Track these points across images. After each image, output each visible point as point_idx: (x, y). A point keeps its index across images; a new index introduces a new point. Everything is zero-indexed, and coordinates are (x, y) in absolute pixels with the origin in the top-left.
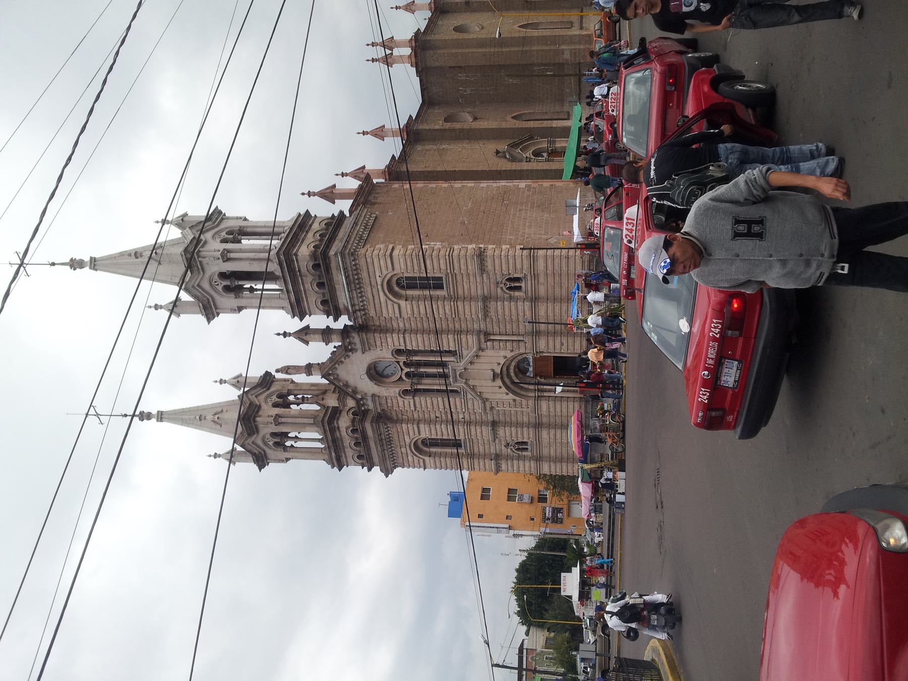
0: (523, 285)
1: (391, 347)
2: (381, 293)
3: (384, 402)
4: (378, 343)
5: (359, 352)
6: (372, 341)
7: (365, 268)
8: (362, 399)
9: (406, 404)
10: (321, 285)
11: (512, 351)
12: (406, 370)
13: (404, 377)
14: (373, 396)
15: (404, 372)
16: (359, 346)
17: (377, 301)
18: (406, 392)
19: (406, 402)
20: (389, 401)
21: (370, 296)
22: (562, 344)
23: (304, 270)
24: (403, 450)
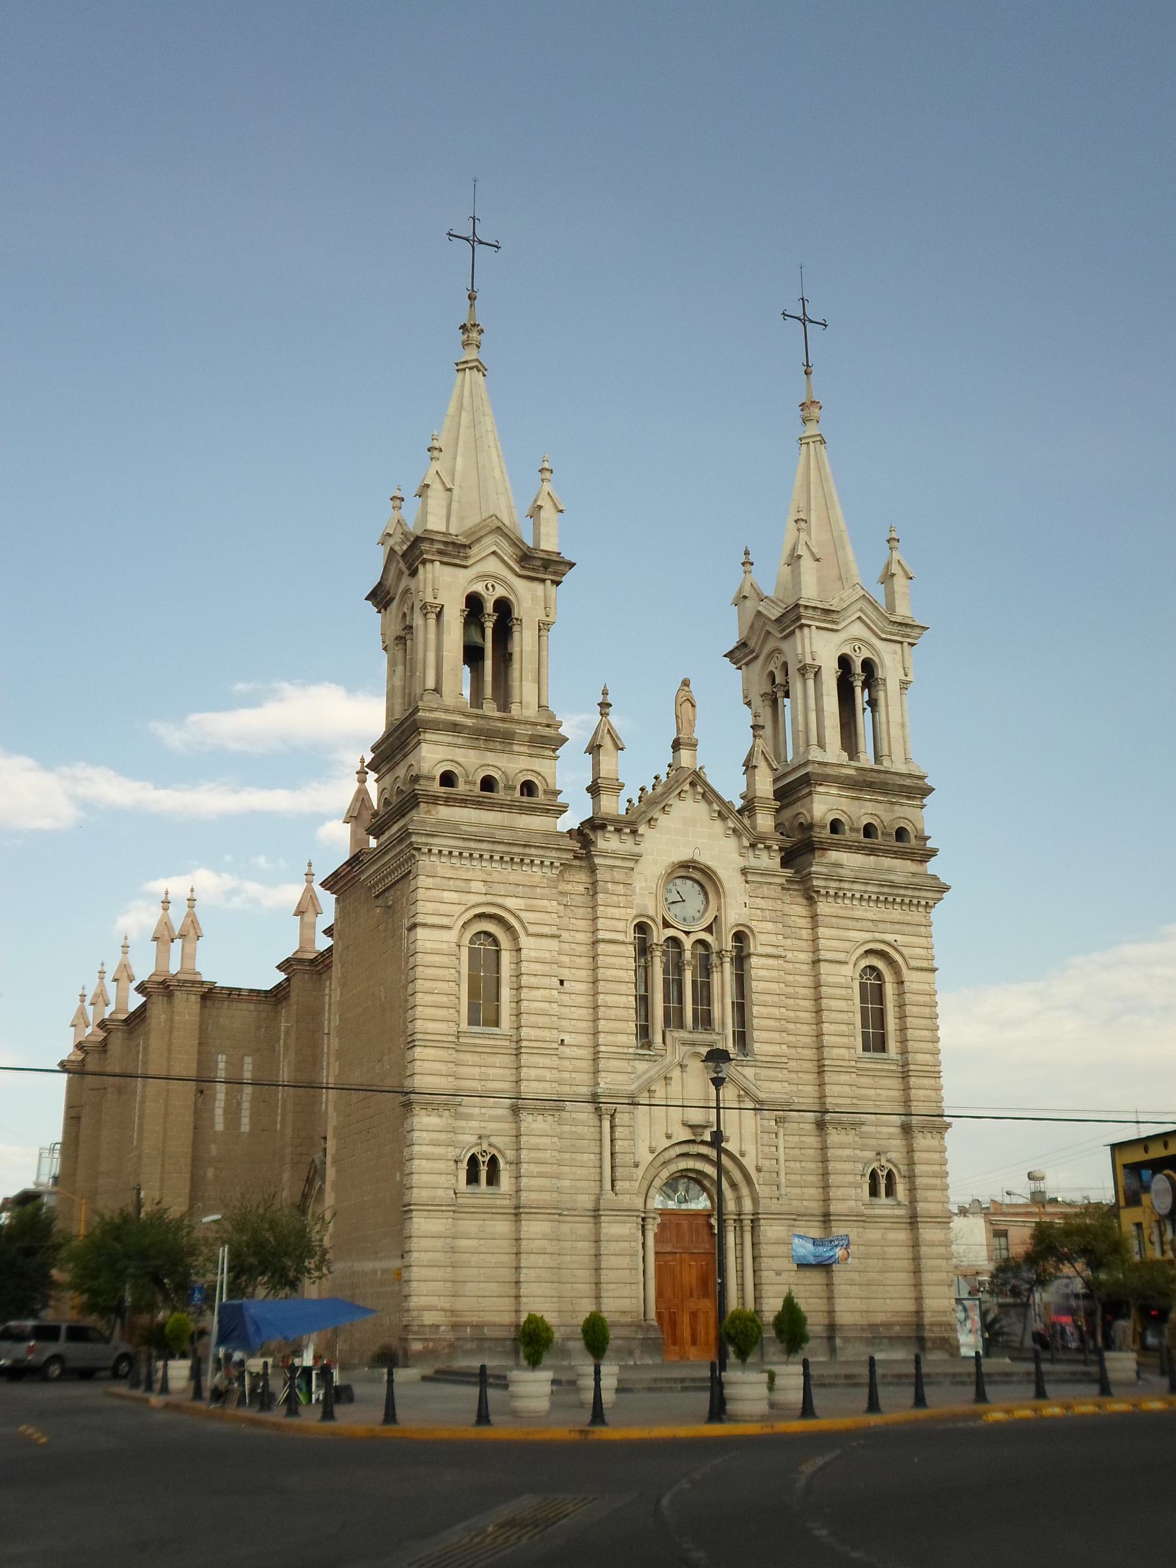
0: (883, 1199)
2: (869, 936)
3: (619, 875)
4: (762, 903)
5: (742, 863)
6: (765, 890)
7: (908, 919)
8: (634, 832)
9: (617, 923)
10: (869, 830)
11: (759, 1170)
12: (688, 943)
13: (670, 932)
14: (636, 858)
15: (682, 936)
16: (752, 862)
17: (851, 923)
18: (641, 928)
19: (621, 925)
20: (620, 889)
21: (859, 913)
22: (778, 1273)
23: (899, 811)
24: (477, 886)
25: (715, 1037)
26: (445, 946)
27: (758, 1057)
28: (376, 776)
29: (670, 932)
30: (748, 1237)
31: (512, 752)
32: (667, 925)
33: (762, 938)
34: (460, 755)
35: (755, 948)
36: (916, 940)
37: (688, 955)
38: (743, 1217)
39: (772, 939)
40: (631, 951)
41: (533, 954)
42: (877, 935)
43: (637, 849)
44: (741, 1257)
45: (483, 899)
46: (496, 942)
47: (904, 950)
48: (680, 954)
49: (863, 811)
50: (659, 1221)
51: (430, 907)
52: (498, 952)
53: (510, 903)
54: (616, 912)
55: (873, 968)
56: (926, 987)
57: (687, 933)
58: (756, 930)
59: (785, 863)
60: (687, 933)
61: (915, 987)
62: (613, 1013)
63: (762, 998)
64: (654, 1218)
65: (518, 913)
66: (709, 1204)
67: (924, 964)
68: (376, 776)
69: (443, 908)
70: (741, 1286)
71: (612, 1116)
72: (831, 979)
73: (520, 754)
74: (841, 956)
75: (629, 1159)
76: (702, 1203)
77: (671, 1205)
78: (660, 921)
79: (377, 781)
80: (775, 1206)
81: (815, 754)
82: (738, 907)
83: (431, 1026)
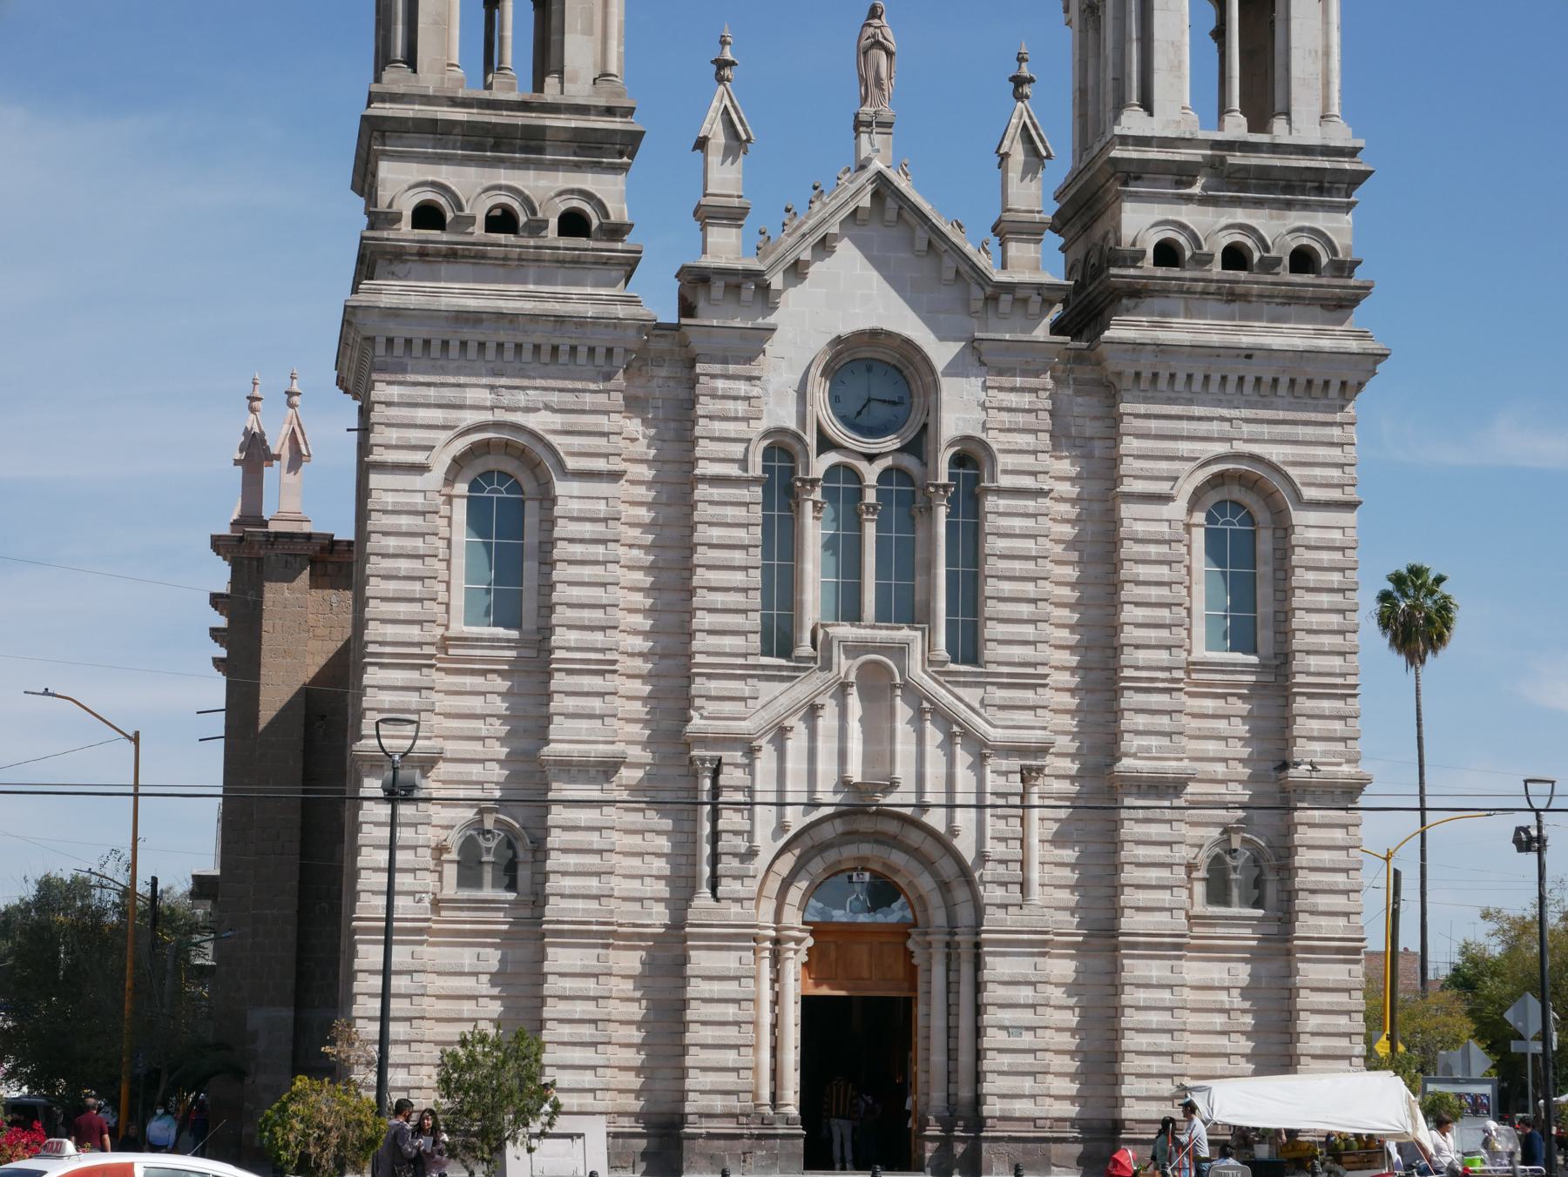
1: (995, 440)
2: (1221, 448)
12: (871, 473)
15: (862, 466)
25: (905, 633)
26: (418, 499)
27: (992, 668)
28: (1061, 241)
29: (832, 458)
30: (966, 970)
31: (540, 166)
32: (826, 444)
33: (1004, 461)
34: (445, 174)
35: (993, 478)
36: (1321, 452)
37: (870, 497)
38: (957, 938)
39: (1027, 461)
40: (758, 492)
41: (575, 506)
42: (1240, 447)
43: (771, 320)
44: (951, 1010)
45: (487, 416)
46: (517, 487)
47: (1293, 472)
48: (859, 494)
49: (1225, 221)
50: (810, 942)
51: (393, 435)
52: (522, 502)
53: (533, 421)
54: (731, 428)
55: (1238, 506)
56: (1336, 535)
57: (871, 458)
58: (995, 447)
59: (1056, 328)
60: (871, 458)
61: (1313, 535)
62: (719, 599)
63: (1003, 565)
64: (799, 941)
65: (551, 438)
66: (908, 914)
67: (1336, 494)
68: (1061, 241)
69: (415, 436)
70: (951, 1054)
71: (716, 772)
72: (1140, 528)
73: (555, 166)
74: (1162, 487)
75: (741, 845)
76: (895, 914)
77: (839, 916)
78: (811, 439)
79: (1063, 249)
80: (1011, 919)
81: (1133, 122)
82: (961, 409)
83: (391, 631)
